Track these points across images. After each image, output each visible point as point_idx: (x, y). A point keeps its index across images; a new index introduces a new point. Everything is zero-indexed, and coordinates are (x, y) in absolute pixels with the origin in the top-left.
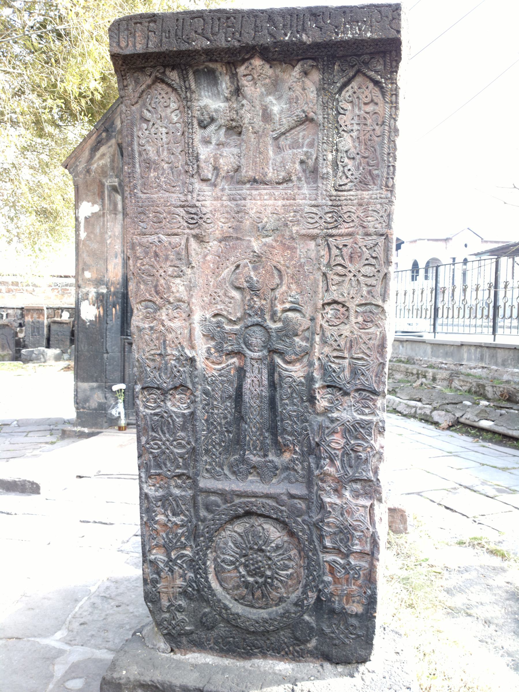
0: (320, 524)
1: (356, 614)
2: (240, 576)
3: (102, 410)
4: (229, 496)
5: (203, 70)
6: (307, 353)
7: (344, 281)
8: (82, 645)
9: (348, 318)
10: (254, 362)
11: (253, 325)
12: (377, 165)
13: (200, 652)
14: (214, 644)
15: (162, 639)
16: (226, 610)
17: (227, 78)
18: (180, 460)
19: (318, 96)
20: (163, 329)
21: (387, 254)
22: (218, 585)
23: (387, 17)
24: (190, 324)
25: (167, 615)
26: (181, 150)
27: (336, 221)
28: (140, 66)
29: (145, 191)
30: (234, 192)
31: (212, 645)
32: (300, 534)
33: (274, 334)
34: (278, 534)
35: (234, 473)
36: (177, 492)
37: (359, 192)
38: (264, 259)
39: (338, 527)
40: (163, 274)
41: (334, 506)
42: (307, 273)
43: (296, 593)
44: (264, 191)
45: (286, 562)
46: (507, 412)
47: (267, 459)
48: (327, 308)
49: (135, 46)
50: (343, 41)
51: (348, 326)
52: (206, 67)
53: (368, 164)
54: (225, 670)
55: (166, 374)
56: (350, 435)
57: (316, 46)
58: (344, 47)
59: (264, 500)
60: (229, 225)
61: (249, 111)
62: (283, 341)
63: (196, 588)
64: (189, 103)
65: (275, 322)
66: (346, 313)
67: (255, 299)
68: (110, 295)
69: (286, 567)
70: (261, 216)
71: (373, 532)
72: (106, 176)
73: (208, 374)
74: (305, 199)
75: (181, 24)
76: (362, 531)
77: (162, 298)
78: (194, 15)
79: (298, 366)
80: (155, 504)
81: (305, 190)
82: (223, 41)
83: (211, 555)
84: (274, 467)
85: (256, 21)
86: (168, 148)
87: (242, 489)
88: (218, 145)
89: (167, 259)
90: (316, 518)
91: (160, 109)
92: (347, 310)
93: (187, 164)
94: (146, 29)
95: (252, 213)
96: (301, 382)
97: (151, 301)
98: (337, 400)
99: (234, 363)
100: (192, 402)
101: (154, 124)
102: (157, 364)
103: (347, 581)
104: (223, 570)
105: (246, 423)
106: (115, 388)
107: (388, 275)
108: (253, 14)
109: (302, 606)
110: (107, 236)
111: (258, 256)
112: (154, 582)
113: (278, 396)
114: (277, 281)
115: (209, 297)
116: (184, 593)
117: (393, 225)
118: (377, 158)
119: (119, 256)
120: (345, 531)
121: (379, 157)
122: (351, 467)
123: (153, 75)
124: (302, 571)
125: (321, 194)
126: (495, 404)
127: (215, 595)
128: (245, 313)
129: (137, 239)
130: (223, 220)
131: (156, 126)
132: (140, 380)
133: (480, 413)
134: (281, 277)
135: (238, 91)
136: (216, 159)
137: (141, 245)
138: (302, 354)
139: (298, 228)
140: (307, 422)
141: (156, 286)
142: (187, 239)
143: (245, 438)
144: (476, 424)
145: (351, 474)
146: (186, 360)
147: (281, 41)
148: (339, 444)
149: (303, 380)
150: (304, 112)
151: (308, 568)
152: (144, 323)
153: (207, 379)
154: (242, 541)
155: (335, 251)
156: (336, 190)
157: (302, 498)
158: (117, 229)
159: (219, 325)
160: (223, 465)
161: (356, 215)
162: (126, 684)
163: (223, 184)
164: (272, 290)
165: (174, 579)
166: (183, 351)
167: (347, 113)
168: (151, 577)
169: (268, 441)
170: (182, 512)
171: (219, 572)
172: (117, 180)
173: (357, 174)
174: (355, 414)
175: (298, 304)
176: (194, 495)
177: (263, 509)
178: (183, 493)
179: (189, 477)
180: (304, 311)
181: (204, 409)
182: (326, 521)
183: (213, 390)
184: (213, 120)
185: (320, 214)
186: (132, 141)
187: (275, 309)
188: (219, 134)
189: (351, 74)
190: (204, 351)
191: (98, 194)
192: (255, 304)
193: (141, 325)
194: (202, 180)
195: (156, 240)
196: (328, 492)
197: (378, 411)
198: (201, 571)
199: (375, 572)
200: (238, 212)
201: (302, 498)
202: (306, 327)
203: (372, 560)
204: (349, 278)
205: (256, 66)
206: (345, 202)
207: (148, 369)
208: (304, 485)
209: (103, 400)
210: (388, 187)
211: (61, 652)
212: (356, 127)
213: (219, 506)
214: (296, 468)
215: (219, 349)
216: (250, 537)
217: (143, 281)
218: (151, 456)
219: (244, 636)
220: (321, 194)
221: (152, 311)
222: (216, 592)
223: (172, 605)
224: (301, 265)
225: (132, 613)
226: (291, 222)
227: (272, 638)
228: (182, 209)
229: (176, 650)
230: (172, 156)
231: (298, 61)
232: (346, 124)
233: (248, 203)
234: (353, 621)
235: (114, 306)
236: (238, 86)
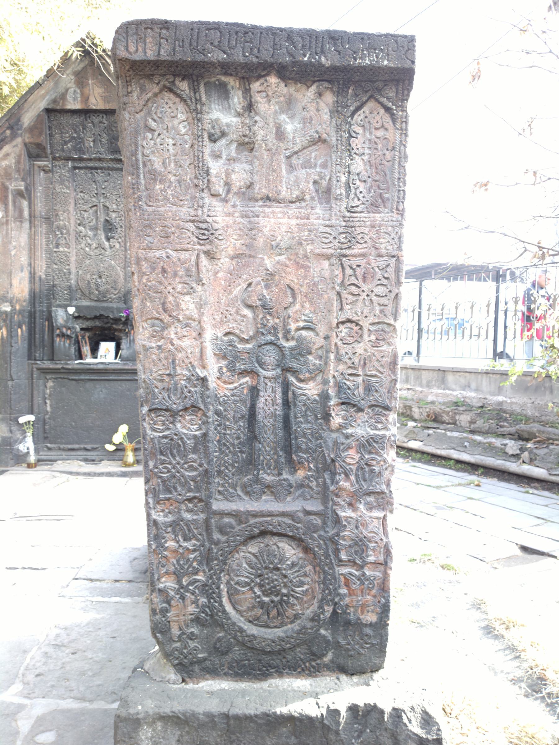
0: (336, 538)
1: (371, 623)
2: (256, 596)
3: (7, 446)
4: (244, 516)
5: (215, 82)
6: (321, 371)
7: (357, 300)
8: (43, 697)
9: (361, 336)
10: (267, 381)
11: (266, 344)
12: (388, 189)
13: (213, 678)
14: (229, 669)
15: (172, 670)
16: (241, 633)
17: (240, 93)
18: (192, 483)
19: (331, 118)
20: (172, 348)
21: (398, 275)
22: (232, 608)
23: (403, 47)
24: (201, 343)
25: (178, 645)
26: (189, 163)
27: (349, 241)
28: (149, 73)
29: (150, 204)
30: (246, 209)
31: (226, 670)
32: (316, 549)
33: (288, 353)
34: (293, 552)
35: (247, 493)
36: (188, 516)
37: (371, 215)
38: (277, 277)
39: (353, 540)
40: (171, 291)
41: (350, 519)
42: (321, 292)
43: (311, 608)
44: (278, 210)
45: (302, 578)
46: (434, 432)
47: (282, 477)
48: (341, 327)
49: (145, 52)
50: (361, 67)
51: (361, 344)
52: (218, 80)
53: (379, 187)
54: (243, 693)
55: (175, 395)
56: (364, 450)
57: (334, 69)
58: (361, 73)
59: (280, 519)
60: (242, 242)
61: (262, 128)
62: (297, 359)
63: (209, 613)
64: (199, 115)
65: (288, 340)
66: (360, 332)
67: (268, 318)
68: (15, 313)
69: (302, 584)
70: (276, 234)
71: (387, 543)
73: (221, 393)
74: (318, 218)
75: (196, 34)
76: (376, 542)
77: (170, 316)
78: (211, 26)
79: (311, 384)
80: (165, 531)
81: (319, 210)
82: (241, 55)
83: (224, 579)
84: (289, 485)
85: (274, 39)
86: (175, 160)
87: (257, 509)
88: (228, 160)
89: (175, 275)
90: (331, 532)
91: (166, 119)
92: (360, 329)
93: (196, 177)
94: (158, 35)
95: (266, 230)
96: (315, 400)
97: (157, 319)
98: (351, 416)
99: (247, 382)
100: (204, 423)
101: (159, 134)
102: (165, 385)
103: (362, 591)
104: (237, 592)
105: (260, 443)
106: (22, 420)
107: (399, 295)
108: (271, 31)
109: (318, 621)
110: (11, 247)
111: (271, 275)
112: (164, 612)
113: (292, 415)
114: (290, 299)
115: (220, 316)
116: (197, 620)
117: (404, 246)
118: (387, 182)
119: (25, 269)
120: (360, 543)
121: (389, 181)
122: (365, 480)
123: (162, 83)
124: (317, 586)
125: (335, 214)
126: (423, 424)
127: (229, 618)
128: (257, 332)
129: (142, 254)
130: (235, 237)
131: (162, 136)
132: (147, 401)
133: (408, 434)
134: (294, 296)
135: (250, 107)
136: (228, 174)
137: (146, 260)
138: (317, 372)
139: (312, 247)
140: (321, 439)
141: (164, 304)
142: (198, 256)
143: (259, 457)
144: (405, 445)
145: (365, 487)
146: (198, 380)
147: (300, 61)
148: (354, 459)
149: (317, 398)
150: (318, 133)
151: (324, 582)
152: (150, 342)
153: (218, 399)
154: (257, 561)
155: (349, 271)
156: (349, 211)
157: (318, 514)
158: (24, 239)
159: (231, 344)
160: (236, 485)
161: (369, 236)
162: (145, 718)
163: (234, 200)
164: (285, 308)
165: (185, 607)
166: (194, 370)
167: (359, 136)
168: (160, 607)
169: (283, 460)
170: (194, 536)
171: (232, 594)
172: (23, 183)
173: (368, 197)
174: (368, 429)
175: (312, 323)
176: (207, 518)
177: (279, 528)
178: (195, 517)
179: (201, 500)
180: (317, 329)
181: (216, 430)
182: (341, 534)
183: (225, 410)
184: (223, 134)
185: (334, 234)
186: (136, 150)
187: (289, 327)
188: (229, 149)
189: (364, 99)
190: (216, 370)
192: (268, 322)
193: (147, 344)
194: (212, 195)
195: (164, 255)
196: (343, 506)
197: (390, 426)
198: (214, 595)
199: (388, 581)
200: (251, 229)
201: (318, 514)
202: (320, 345)
203: (385, 570)
204: (363, 297)
205: (271, 84)
206: (358, 224)
207: (156, 390)
208: (319, 501)
209: (8, 435)
210: (399, 211)
211: (21, 707)
212: (367, 151)
213: (233, 528)
214: (311, 484)
215: (231, 368)
216: (265, 557)
217: (150, 298)
218: (160, 481)
219: (260, 658)
220: (335, 214)
221: (159, 329)
222: (230, 615)
223: (183, 634)
224: (314, 284)
225: (91, 659)
226: (305, 241)
227: (288, 656)
228: (191, 224)
229: (188, 680)
230: (180, 169)
231: (314, 82)
232: (358, 147)
233: (262, 221)
234: (368, 631)
235: (20, 326)
236: (251, 101)
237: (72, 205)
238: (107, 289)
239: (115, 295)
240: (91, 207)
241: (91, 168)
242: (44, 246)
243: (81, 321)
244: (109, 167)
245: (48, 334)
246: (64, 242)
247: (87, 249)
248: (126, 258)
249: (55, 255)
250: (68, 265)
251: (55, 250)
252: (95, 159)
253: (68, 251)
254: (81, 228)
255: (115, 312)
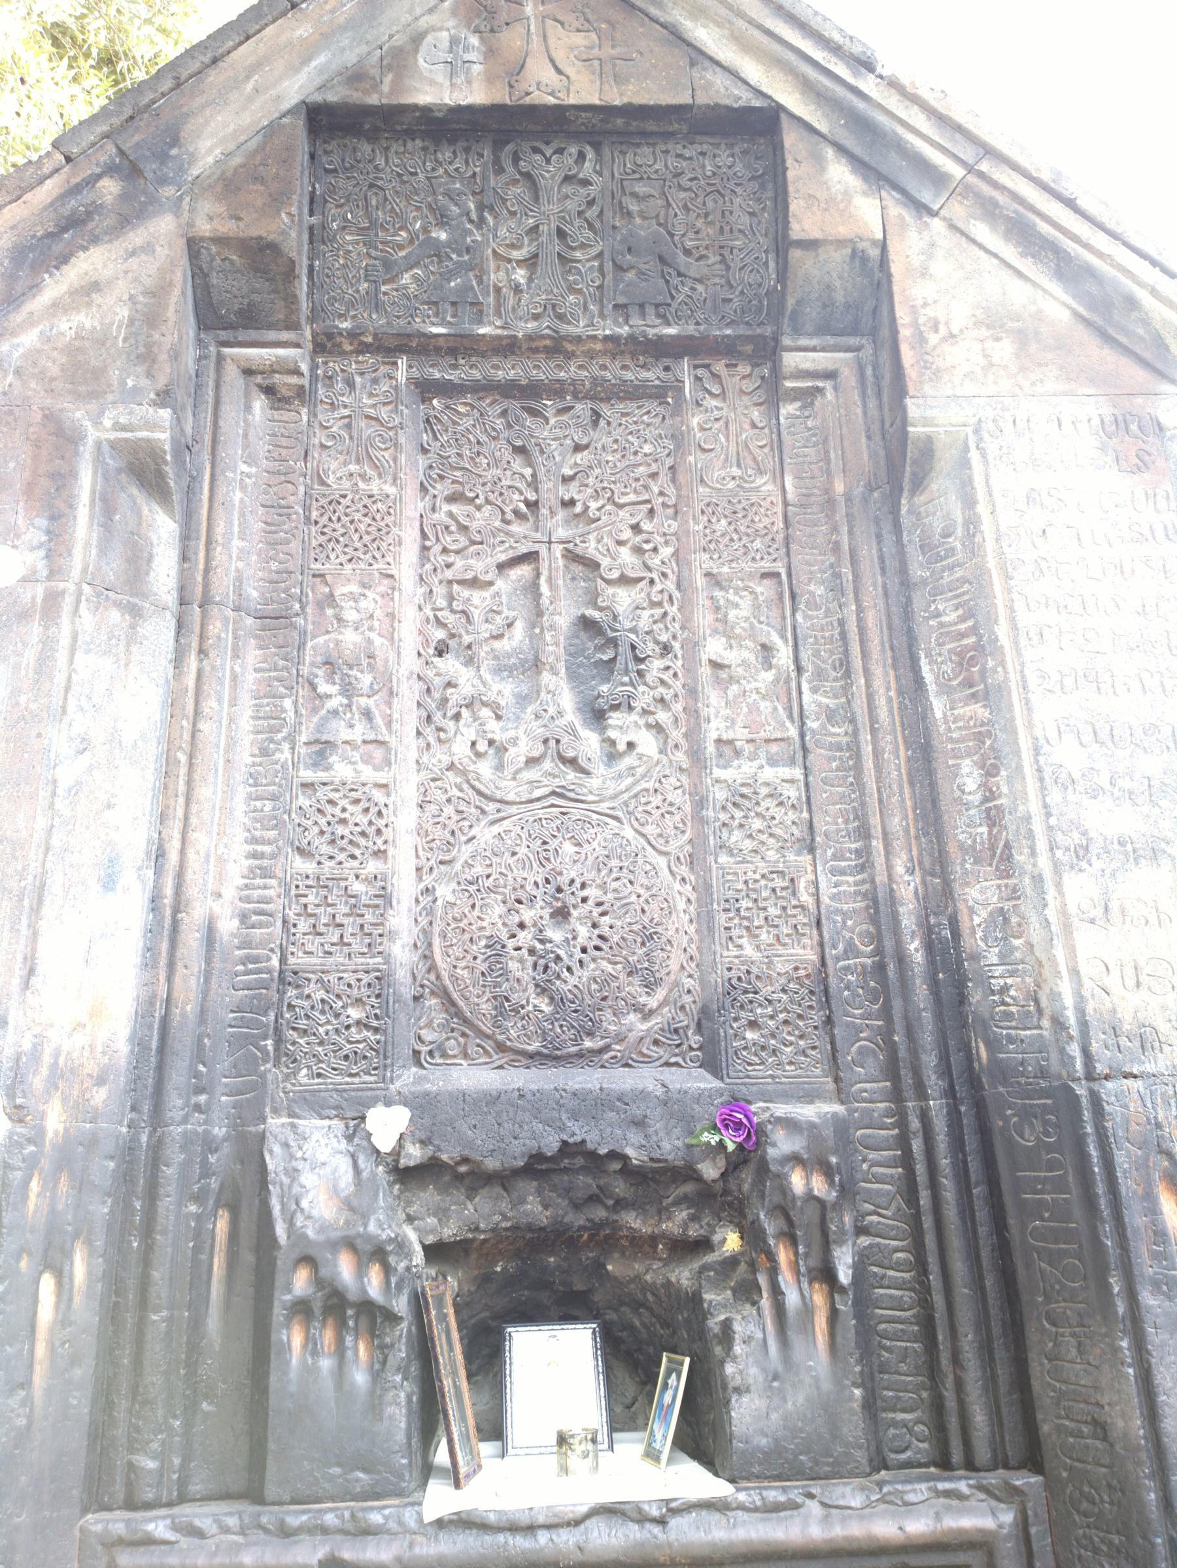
68: (31, 1164)
72: (94, 395)
172: (165, 414)
191: (29, 489)
237: (409, 553)
238: (606, 981)
239: (647, 1015)
240: (501, 567)
241: (508, 390)
242: (245, 755)
243: (429, 1196)
244: (594, 380)
245: (227, 1305)
246: (359, 732)
247: (485, 769)
248: (700, 803)
249: (303, 801)
250: (380, 854)
251: (307, 775)
252: (529, 347)
253: (382, 777)
254: (450, 665)
255: (657, 1125)
